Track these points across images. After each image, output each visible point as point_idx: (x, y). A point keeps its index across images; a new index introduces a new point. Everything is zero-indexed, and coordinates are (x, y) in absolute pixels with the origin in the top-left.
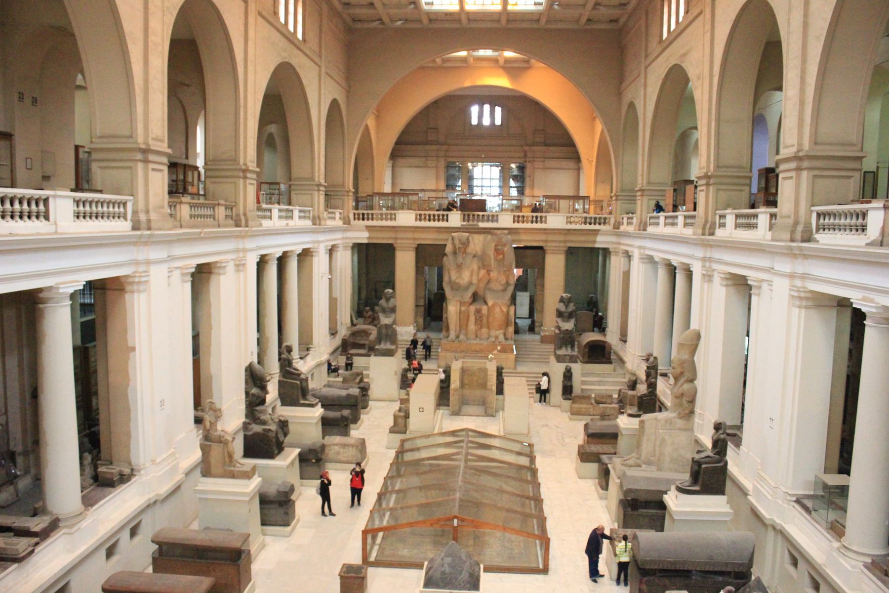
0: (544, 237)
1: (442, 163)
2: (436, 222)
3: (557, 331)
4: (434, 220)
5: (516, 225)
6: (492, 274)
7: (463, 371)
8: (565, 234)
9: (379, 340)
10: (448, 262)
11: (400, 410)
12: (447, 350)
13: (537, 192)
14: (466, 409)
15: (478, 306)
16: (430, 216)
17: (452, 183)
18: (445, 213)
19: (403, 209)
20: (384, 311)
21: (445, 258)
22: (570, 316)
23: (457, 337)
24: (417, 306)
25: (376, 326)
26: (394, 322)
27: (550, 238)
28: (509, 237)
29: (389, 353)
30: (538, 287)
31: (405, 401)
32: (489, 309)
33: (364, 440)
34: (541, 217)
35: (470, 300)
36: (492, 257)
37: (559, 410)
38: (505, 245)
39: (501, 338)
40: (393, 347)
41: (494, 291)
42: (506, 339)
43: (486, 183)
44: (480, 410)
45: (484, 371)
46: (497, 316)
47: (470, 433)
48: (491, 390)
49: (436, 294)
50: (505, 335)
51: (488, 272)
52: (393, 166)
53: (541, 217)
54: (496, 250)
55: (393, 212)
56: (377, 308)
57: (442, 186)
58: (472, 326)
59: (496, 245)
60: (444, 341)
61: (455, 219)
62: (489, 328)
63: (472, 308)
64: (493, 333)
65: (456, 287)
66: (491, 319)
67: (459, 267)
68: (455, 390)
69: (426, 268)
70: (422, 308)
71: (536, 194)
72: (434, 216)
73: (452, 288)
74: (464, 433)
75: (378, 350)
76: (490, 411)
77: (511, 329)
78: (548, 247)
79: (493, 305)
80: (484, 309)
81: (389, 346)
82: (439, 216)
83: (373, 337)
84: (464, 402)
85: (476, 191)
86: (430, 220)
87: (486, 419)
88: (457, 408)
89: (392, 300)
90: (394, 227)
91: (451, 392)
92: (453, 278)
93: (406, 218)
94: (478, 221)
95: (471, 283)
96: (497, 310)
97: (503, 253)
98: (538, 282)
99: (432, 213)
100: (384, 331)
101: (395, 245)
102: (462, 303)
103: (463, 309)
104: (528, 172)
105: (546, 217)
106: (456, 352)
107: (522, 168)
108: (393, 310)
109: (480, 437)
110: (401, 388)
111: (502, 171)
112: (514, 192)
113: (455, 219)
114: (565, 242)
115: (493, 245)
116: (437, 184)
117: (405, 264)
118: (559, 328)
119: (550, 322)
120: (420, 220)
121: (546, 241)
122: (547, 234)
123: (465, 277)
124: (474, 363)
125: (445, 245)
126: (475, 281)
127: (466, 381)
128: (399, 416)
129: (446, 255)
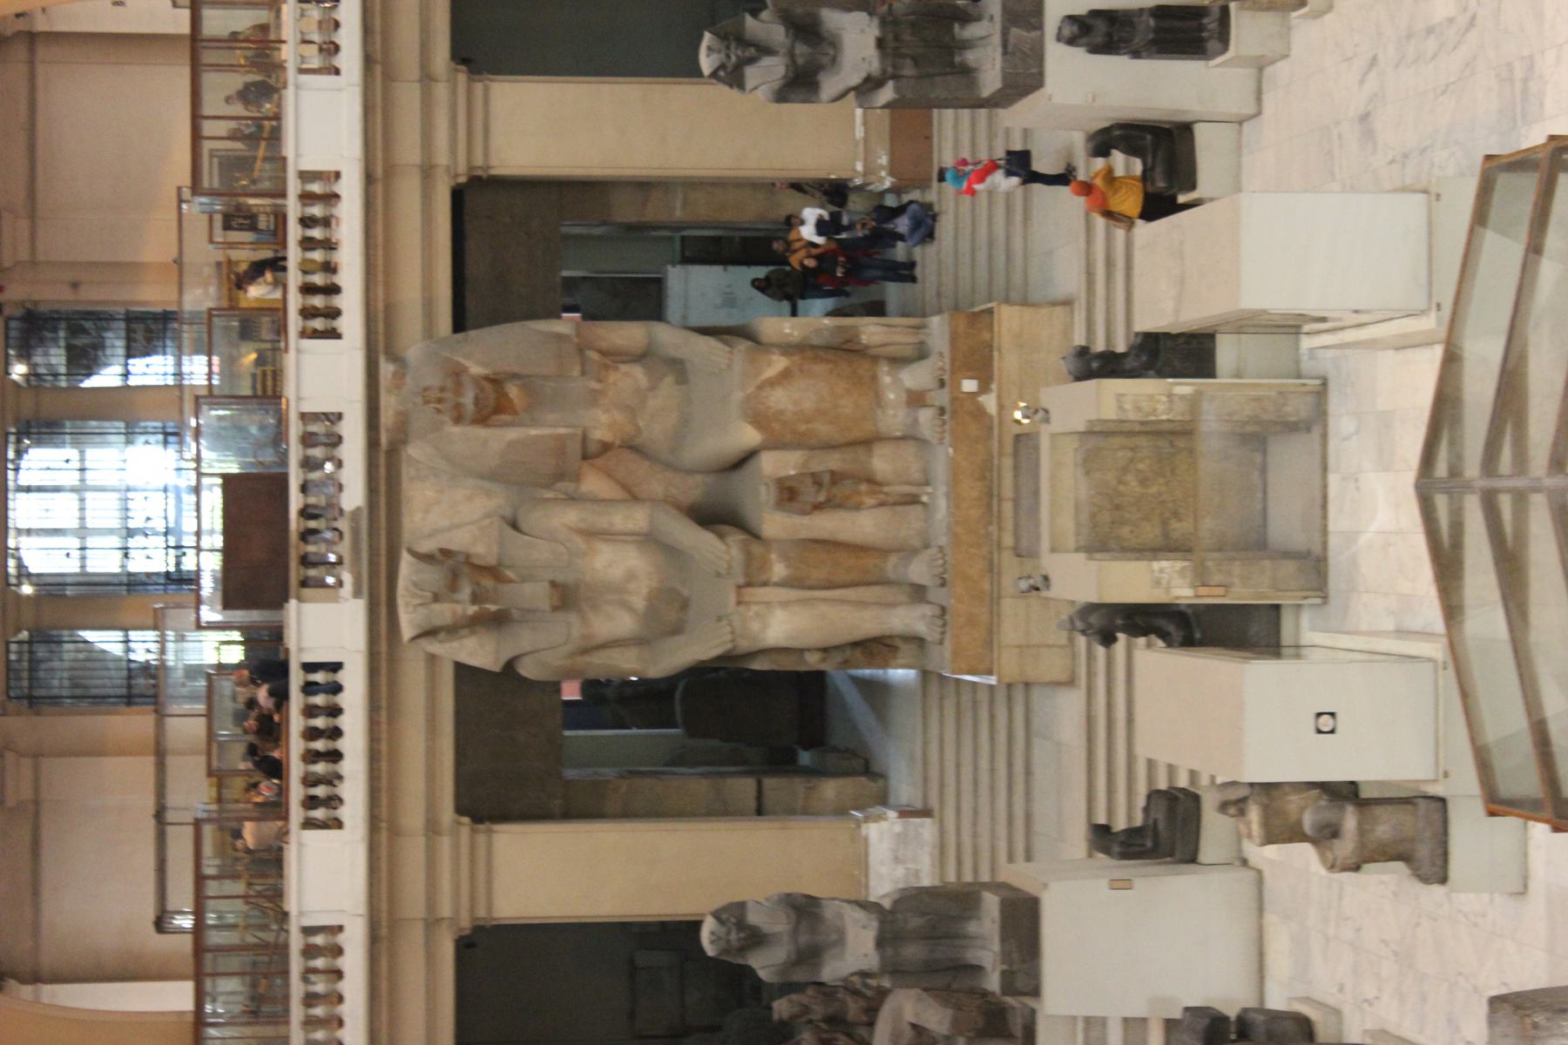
0: (408, 192)
1: (20, 726)
2: (344, 722)
3: (887, 94)
4: (336, 733)
5: (352, 322)
6: (599, 434)
7: (1100, 544)
8: (389, 77)
9: (947, 975)
10: (545, 649)
11: (1326, 835)
12: (989, 642)
13: (156, 247)
14: (1286, 525)
15: (766, 495)
16: (311, 757)
17: (119, 677)
18: (296, 678)
19: (277, 895)
20: (810, 955)
21: (527, 670)
22: (806, 30)
23: (918, 593)
24: (760, 811)
25: (872, 1012)
26: (864, 905)
27: (409, 151)
28: (414, 349)
29: (1023, 917)
30: (652, 214)
31: (1278, 809)
32: (775, 444)
33: (1496, 1002)
34: (307, 198)
35: (736, 538)
36: (512, 434)
37: (1281, 70)
38: (457, 373)
39: (916, 377)
40: (991, 904)
41: (685, 421)
42: (921, 354)
43: (103, 511)
44: (1289, 461)
45: (1098, 433)
46: (809, 404)
47: (1441, 469)
48: (1194, 402)
49: (692, 732)
50: (898, 361)
51: (593, 453)
52: (36, 978)
53: (307, 198)
54: (482, 419)
55: (296, 942)
56: (782, 1008)
57: (136, 724)
58: (863, 525)
59: (458, 419)
60: (942, 659)
61: (326, 627)
62: (868, 443)
63: (775, 524)
64: (894, 418)
65: (669, 612)
66: (823, 429)
67: (566, 597)
68: (1201, 578)
69: (570, 773)
70: (770, 783)
71: (166, 240)
72: (311, 734)
73: (677, 630)
74: (1441, 502)
75: (1008, 978)
76: (1298, 408)
77: (871, 330)
78: (451, 164)
79: (758, 419)
80: (777, 464)
81: (988, 922)
82: (310, 712)
83: (937, 1019)
84: (1254, 544)
85: (151, 559)
86: (335, 756)
87: (1341, 422)
88: (1289, 567)
89: (753, 918)
90: (374, 938)
91: (1212, 597)
92: (623, 623)
93: (327, 876)
94: (332, 509)
95: (649, 540)
96: (779, 399)
97: (496, 381)
98: (625, 210)
99: (296, 745)
100: (913, 952)
101: (465, 923)
102: (753, 578)
103: (779, 570)
104: (52, 294)
105: (306, 176)
106: (994, 600)
107: (33, 328)
108: (804, 909)
109: (1456, 421)
110: (1192, 859)
111: (43, 426)
112: (152, 370)
113: (326, 627)
114: (427, 78)
115: (455, 430)
116: (122, 752)
117: (560, 873)
118: (870, 85)
119: (837, 138)
120: (333, 801)
121: (427, 172)
122: (390, 171)
123: (619, 565)
124: (1062, 490)
125: (461, 670)
126: (636, 518)
127: (1150, 532)
128: (1361, 832)
129: (510, 666)
